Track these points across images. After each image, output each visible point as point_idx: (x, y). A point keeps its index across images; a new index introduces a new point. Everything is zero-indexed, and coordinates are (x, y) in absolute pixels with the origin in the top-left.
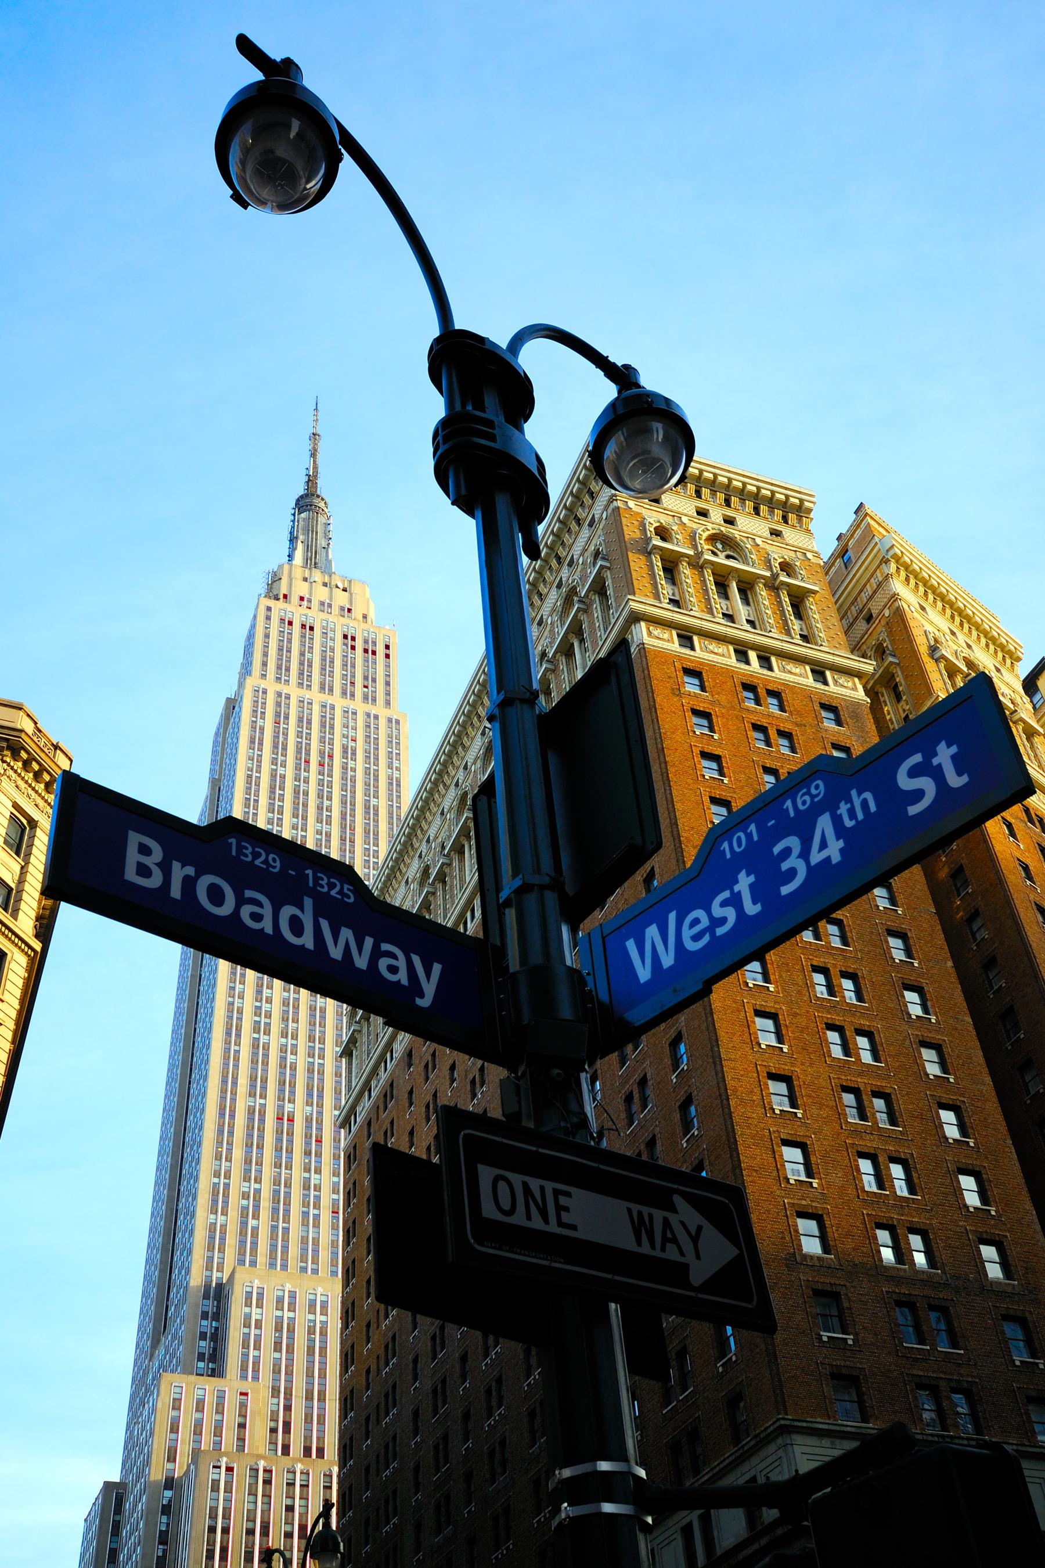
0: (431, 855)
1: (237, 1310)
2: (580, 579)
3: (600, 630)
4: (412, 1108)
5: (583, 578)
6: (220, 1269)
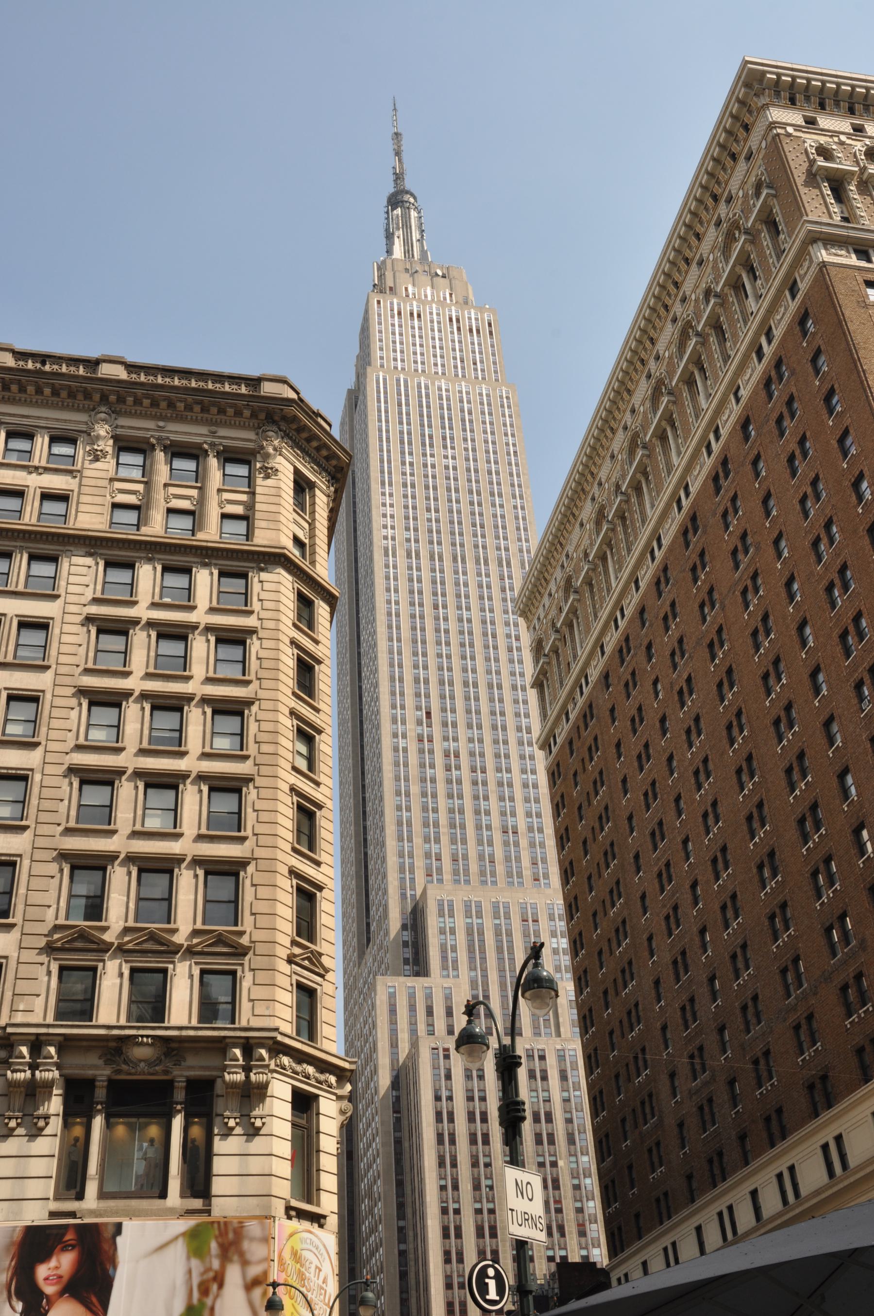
0: (605, 495)
1: (432, 923)
2: (742, 211)
3: (771, 257)
4: (616, 723)
5: (746, 211)
6: (413, 888)
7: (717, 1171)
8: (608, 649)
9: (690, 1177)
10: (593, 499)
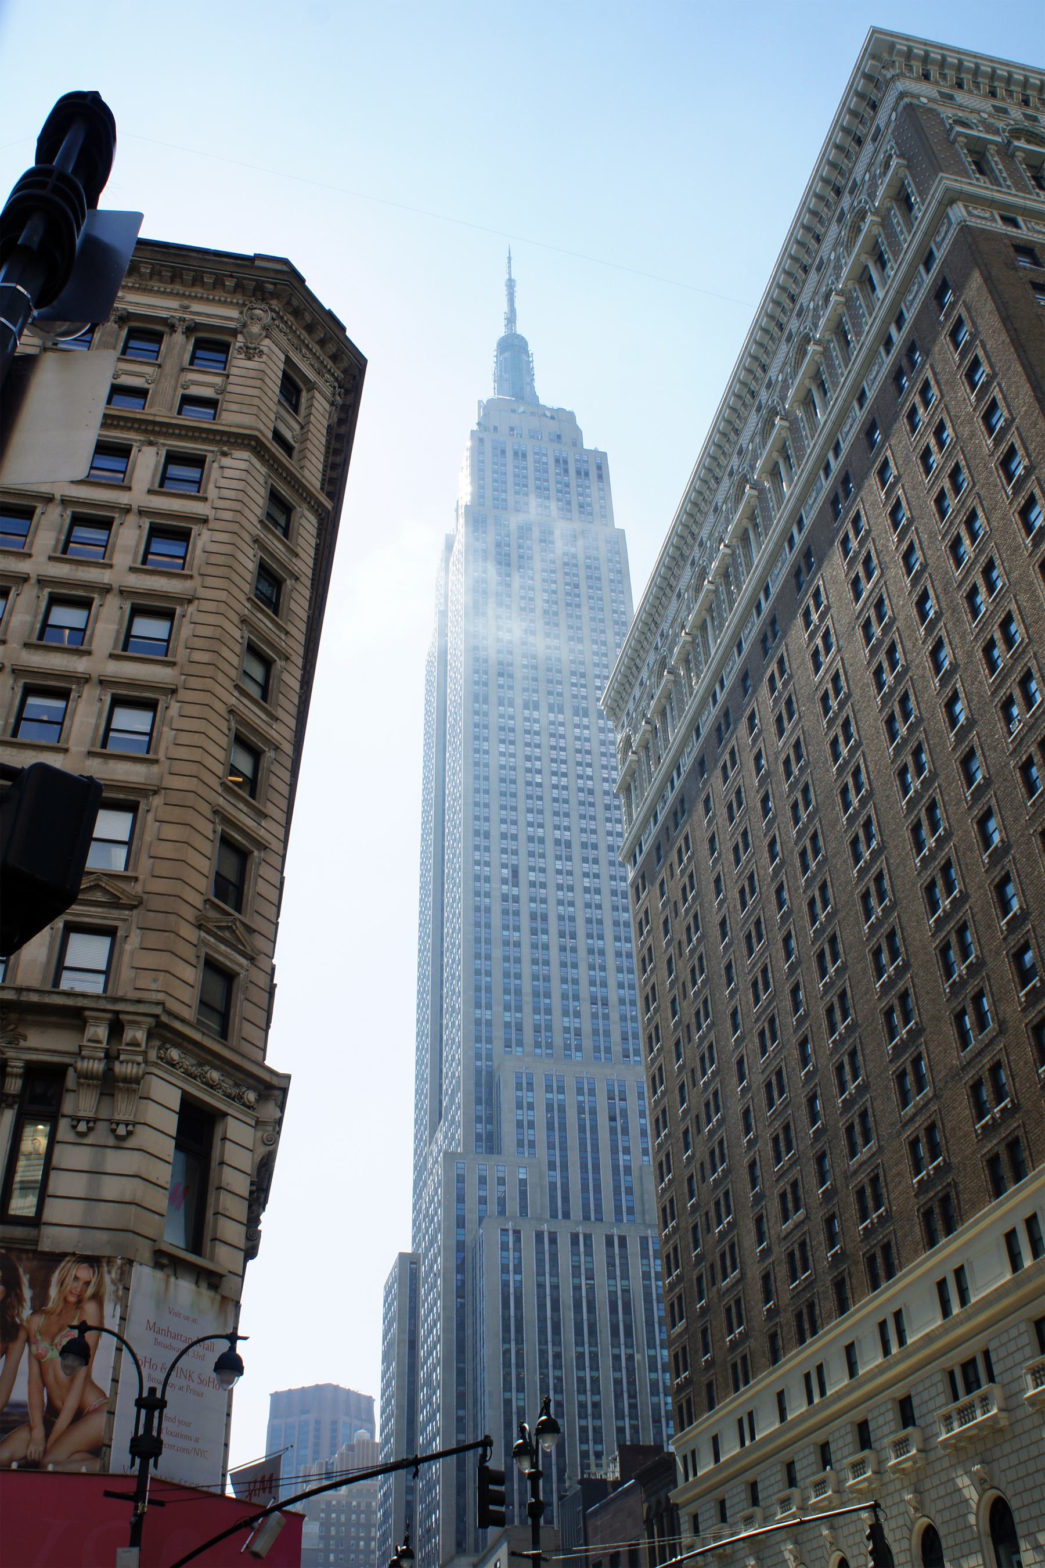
7: (807, 1326)
8: (704, 732)
9: (773, 1337)
10: (693, 564)
